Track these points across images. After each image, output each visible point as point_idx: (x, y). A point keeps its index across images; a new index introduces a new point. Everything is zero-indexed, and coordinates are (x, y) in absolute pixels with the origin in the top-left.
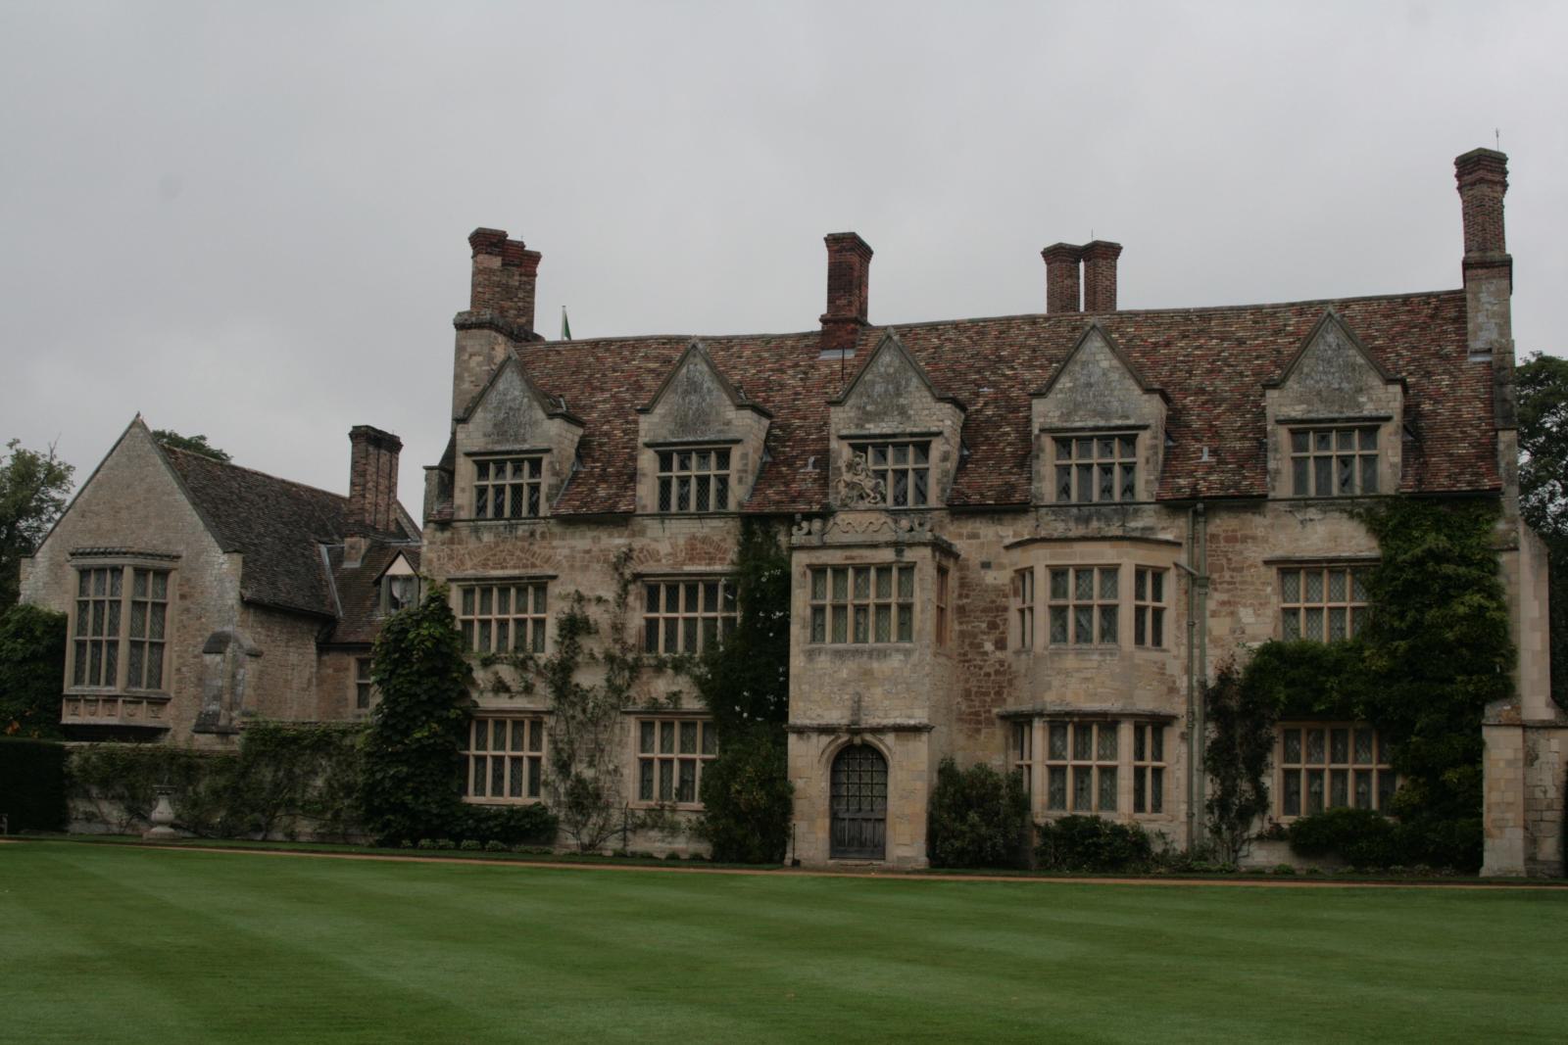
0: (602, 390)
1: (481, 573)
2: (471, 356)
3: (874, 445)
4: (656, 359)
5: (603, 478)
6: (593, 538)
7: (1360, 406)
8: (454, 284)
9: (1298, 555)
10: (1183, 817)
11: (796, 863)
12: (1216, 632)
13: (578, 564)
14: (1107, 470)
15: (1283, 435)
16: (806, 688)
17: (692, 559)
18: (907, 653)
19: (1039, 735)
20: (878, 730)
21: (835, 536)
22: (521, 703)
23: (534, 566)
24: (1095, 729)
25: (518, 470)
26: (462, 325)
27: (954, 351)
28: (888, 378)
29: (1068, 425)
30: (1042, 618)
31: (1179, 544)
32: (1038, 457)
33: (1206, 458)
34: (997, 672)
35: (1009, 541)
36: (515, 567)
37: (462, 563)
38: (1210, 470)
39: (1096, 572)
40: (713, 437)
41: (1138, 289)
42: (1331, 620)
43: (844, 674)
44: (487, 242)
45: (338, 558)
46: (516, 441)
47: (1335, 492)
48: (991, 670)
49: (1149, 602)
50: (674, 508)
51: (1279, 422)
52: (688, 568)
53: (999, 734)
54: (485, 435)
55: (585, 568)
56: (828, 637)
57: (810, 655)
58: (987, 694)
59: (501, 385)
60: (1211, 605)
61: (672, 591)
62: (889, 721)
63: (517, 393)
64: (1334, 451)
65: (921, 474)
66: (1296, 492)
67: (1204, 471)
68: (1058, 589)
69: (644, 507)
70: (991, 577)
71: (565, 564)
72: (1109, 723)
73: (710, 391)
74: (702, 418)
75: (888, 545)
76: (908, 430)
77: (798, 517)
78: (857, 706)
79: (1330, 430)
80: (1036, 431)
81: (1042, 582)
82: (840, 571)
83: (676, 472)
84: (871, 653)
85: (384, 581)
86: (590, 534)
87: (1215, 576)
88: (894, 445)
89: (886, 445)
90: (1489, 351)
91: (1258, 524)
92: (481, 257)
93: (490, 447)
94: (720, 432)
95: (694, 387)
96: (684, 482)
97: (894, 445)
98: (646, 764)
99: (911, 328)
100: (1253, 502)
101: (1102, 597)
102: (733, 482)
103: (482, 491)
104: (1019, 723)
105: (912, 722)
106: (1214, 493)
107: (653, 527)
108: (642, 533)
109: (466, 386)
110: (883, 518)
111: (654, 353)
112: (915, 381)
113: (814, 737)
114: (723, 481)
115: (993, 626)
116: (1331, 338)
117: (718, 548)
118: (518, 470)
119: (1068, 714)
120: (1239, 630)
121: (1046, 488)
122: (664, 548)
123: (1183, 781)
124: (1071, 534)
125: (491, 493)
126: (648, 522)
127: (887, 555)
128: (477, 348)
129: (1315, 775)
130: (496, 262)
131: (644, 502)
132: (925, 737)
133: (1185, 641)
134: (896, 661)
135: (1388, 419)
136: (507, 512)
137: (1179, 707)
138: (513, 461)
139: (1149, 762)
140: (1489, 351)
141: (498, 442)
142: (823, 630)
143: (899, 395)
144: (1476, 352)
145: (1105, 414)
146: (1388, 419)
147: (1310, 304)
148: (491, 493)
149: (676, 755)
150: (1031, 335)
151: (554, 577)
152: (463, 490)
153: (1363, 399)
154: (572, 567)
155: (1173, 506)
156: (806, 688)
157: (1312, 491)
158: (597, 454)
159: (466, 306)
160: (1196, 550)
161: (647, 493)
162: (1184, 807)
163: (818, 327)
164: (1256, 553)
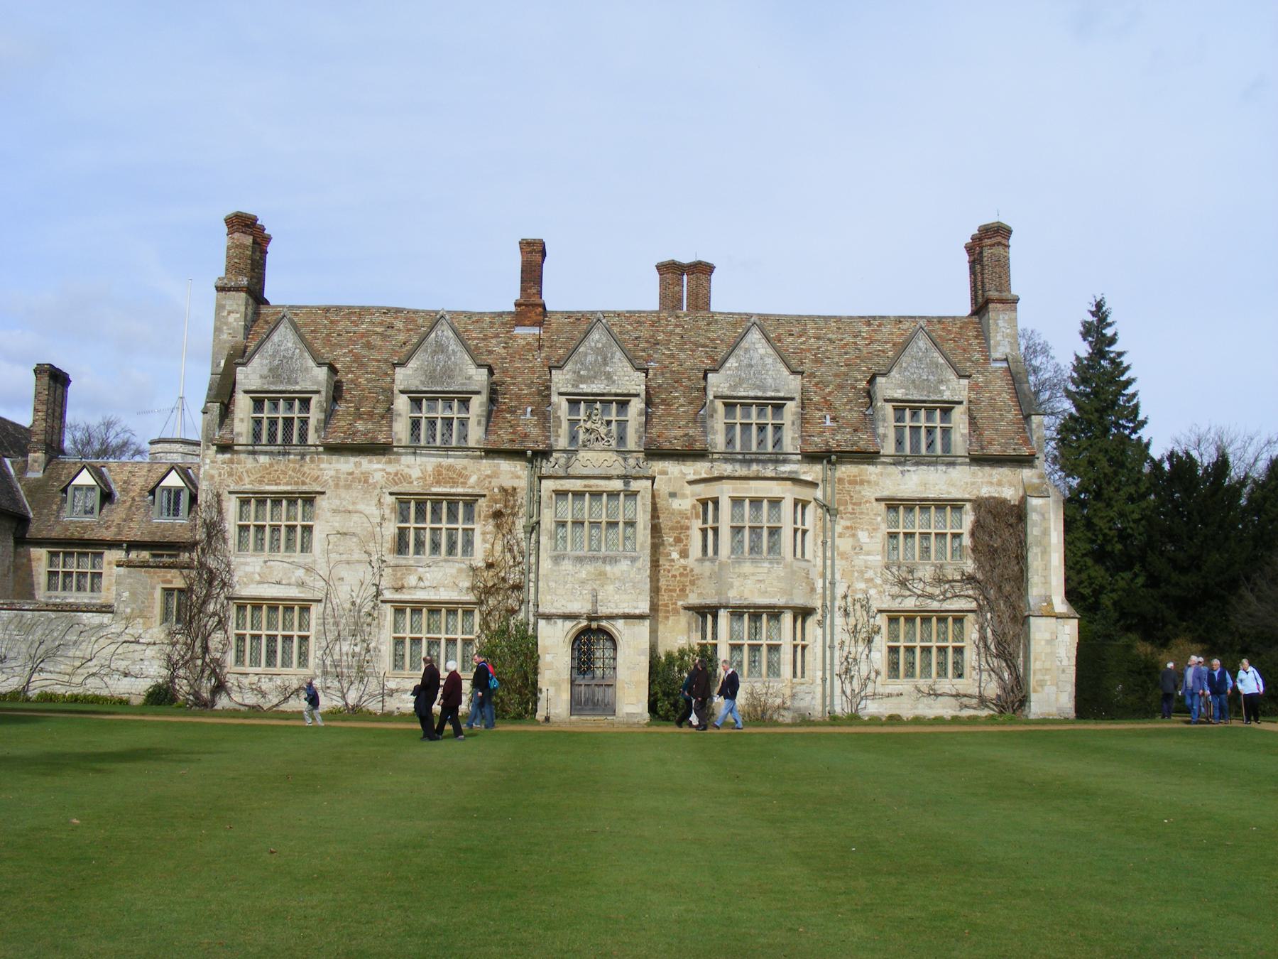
0: (341, 347)
1: (257, 487)
2: (229, 313)
3: (585, 401)
4: (381, 324)
5: (358, 416)
6: (355, 463)
7: (941, 392)
8: (215, 253)
9: (900, 495)
10: (819, 681)
11: (547, 719)
12: (842, 549)
13: (342, 483)
14: (762, 428)
15: (889, 407)
16: (553, 584)
17: (438, 483)
18: (633, 560)
21: (576, 469)
22: (294, 592)
23: (304, 483)
24: (764, 616)
25: (290, 407)
26: (220, 289)
27: (621, 333)
28: (598, 351)
29: (735, 394)
31: (814, 485)
32: (712, 416)
33: (828, 423)
34: (681, 575)
35: (691, 477)
36: (287, 484)
37: (241, 479)
38: (834, 432)
39: (765, 502)
40: (457, 388)
41: (726, 296)
42: (921, 542)
43: (583, 575)
44: (242, 224)
45: (23, 469)
46: (289, 382)
47: (923, 451)
48: (677, 573)
49: (799, 525)
50: (423, 443)
51: (886, 401)
52: (434, 490)
53: (684, 619)
54: (261, 377)
55: (348, 487)
56: (569, 548)
57: (557, 559)
58: (674, 591)
59: (276, 337)
60: (838, 529)
61: (420, 505)
62: (620, 611)
63: (290, 345)
64: (922, 422)
65: (622, 424)
66: (897, 450)
67: (829, 435)
69: (399, 440)
70: (676, 504)
71: (331, 483)
72: (775, 613)
73: (454, 352)
74: (448, 373)
75: (619, 477)
76: (613, 391)
77: (529, 453)
78: (595, 602)
79: (920, 408)
80: (711, 397)
82: (578, 495)
83: (425, 414)
84: (604, 560)
85: (70, 489)
86: (353, 460)
87: (841, 508)
88: (601, 402)
89: (595, 401)
90: (1006, 360)
91: (871, 471)
92: (236, 235)
93: (266, 387)
94: (463, 384)
95: (441, 348)
96: (432, 422)
97: (601, 402)
98: (399, 642)
99: (584, 314)
100: (870, 457)
101: (769, 521)
102: (472, 424)
103: (258, 422)
104: (706, 612)
105: (637, 612)
106: (844, 448)
107: (407, 460)
108: (398, 461)
109: (225, 337)
110: (614, 456)
111: (378, 320)
112: (619, 354)
113: (560, 622)
114: (463, 422)
115: (678, 540)
116: (921, 344)
117: (460, 475)
118: (290, 407)
119: (746, 607)
120: (858, 548)
121: (718, 440)
122: (415, 473)
123: (820, 654)
124: (737, 474)
125: (265, 423)
126: (401, 450)
127: (617, 485)
128: (235, 307)
129: (910, 650)
130: (249, 240)
131: (399, 436)
132: (647, 622)
133: (820, 554)
134: (624, 565)
135: (960, 403)
136: (279, 440)
137: (818, 603)
138: (285, 399)
139: (799, 641)
140: (1006, 360)
141: (272, 383)
142: (565, 542)
143: (605, 364)
144: (996, 360)
145: (764, 389)
146: (960, 403)
147: (874, 318)
148: (265, 423)
150: (677, 326)
151: (323, 493)
152: (242, 420)
153: (943, 388)
154: (337, 486)
155: (811, 457)
156: (553, 584)
157: (908, 451)
158: (348, 397)
159: (223, 274)
160: (829, 490)
161: (401, 430)
162: (820, 674)
163: (513, 309)
164: (870, 493)
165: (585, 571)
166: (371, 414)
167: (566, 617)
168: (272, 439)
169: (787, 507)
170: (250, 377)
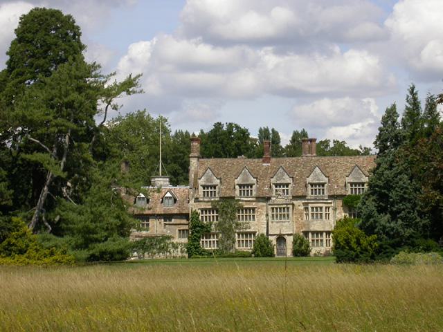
14: (319, 190)
15: (349, 185)
19: (310, 235)
20: (284, 235)
30: (310, 215)
38: (338, 189)
60: (337, 212)
68: (313, 210)
72: (321, 233)
74: (247, 180)
81: (310, 209)
82: (277, 208)
95: (245, 173)
114: (251, 190)
125: (206, 193)
134: (287, 223)
145: (319, 180)
149: (244, 239)
161: (237, 193)
165: (279, 224)
166: (230, 189)
167: (274, 235)
168: (208, 195)
169: (324, 209)
170: (202, 182)
